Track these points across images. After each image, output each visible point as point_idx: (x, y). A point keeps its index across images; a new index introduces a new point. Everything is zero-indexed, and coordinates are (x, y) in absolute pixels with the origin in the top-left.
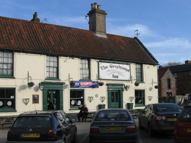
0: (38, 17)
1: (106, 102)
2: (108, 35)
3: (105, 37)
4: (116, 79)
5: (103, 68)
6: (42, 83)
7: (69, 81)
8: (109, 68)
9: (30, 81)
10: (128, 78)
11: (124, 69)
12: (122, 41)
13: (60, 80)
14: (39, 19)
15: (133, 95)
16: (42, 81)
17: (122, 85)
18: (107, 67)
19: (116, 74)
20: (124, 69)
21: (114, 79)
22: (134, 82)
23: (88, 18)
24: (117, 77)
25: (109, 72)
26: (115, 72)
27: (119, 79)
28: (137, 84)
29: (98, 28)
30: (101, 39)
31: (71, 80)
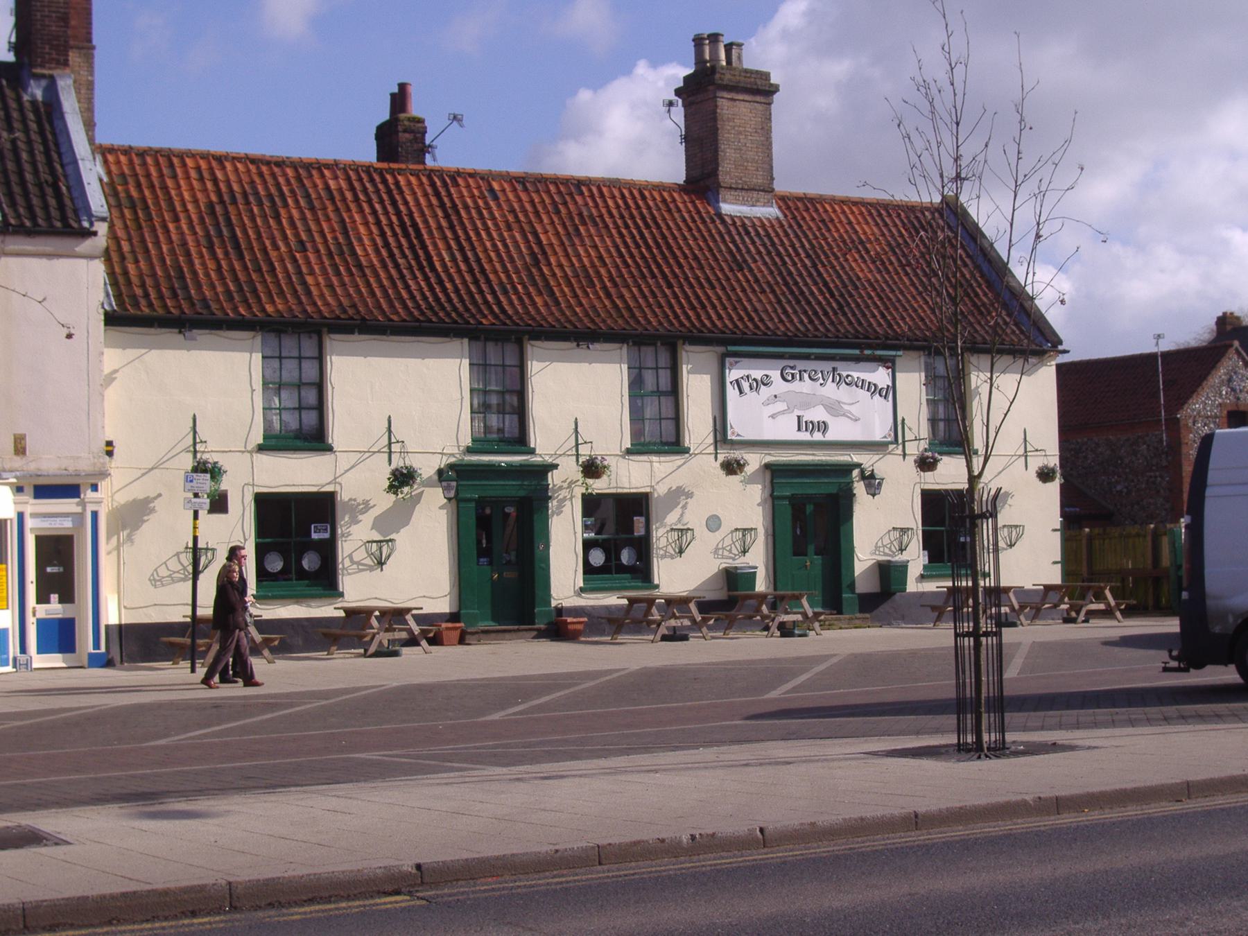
0: (416, 108)
1: (757, 559)
2: (785, 201)
3: (771, 212)
4: (818, 436)
5: (745, 385)
6: (451, 467)
7: (578, 455)
8: (779, 385)
9: (397, 462)
10: (879, 430)
11: (862, 384)
12: (867, 230)
13: (532, 452)
14: (421, 121)
15: (912, 517)
16: (452, 460)
17: (846, 469)
18: (766, 382)
19: (816, 414)
20: (862, 384)
21: (804, 436)
22: (914, 449)
23: (679, 113)
24: (823, 427)
25: (780, 406)
26: (807, 406)
27: (831, 436)
28: (925, 464)
29: (727, 171)
30: (743, 226)
31: (585, 451)
